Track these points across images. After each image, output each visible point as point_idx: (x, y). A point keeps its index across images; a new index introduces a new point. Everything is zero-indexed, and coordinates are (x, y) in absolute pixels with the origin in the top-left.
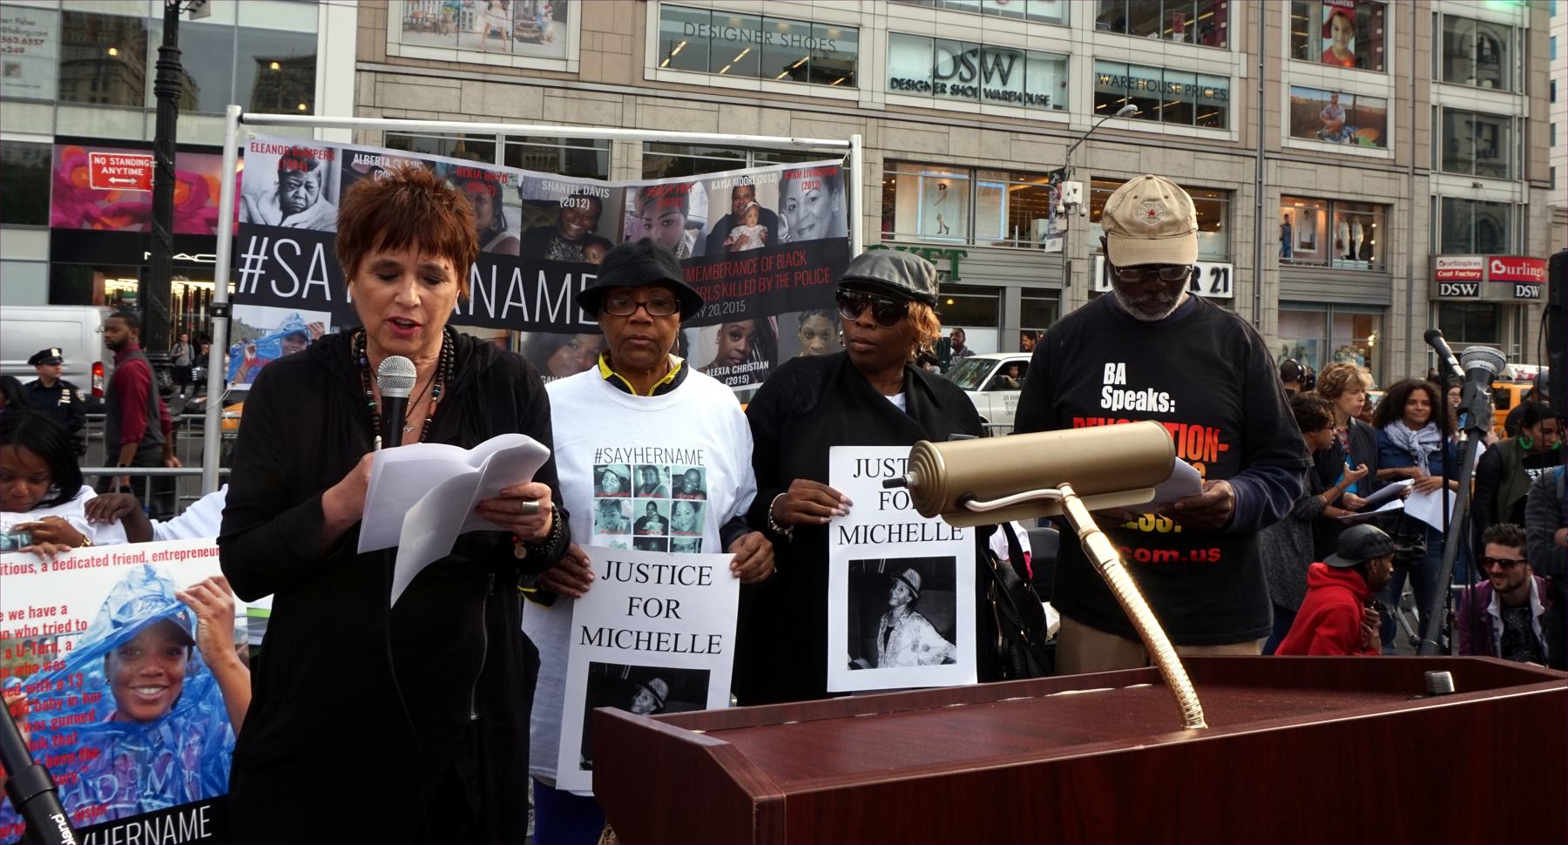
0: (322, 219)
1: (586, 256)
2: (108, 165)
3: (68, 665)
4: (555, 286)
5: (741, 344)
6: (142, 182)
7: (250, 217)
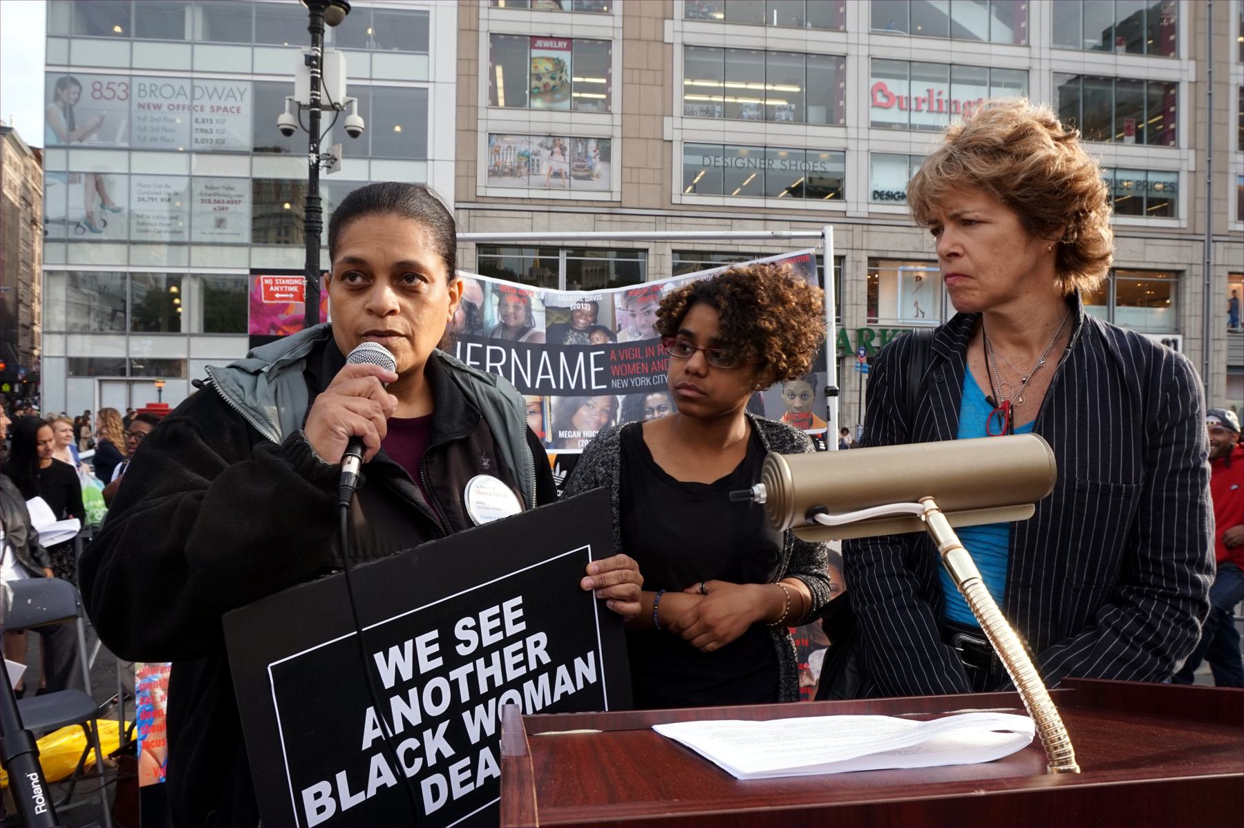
2: (274, 285)
6: (298, 297)
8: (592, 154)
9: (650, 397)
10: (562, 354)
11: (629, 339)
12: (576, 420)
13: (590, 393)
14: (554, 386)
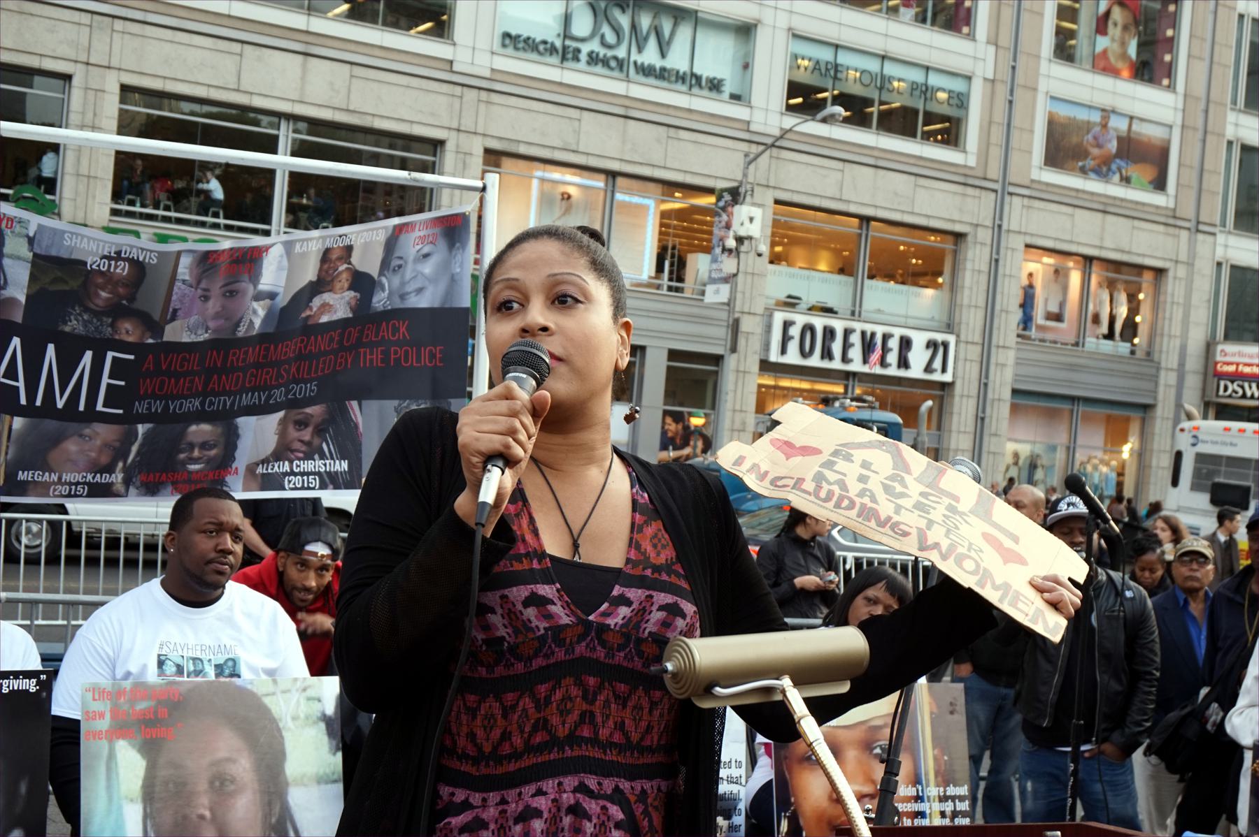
1: (115, 330)
4: (67, 365)
5: (307, 434)
13: (91, 416)
14: (23, 401)
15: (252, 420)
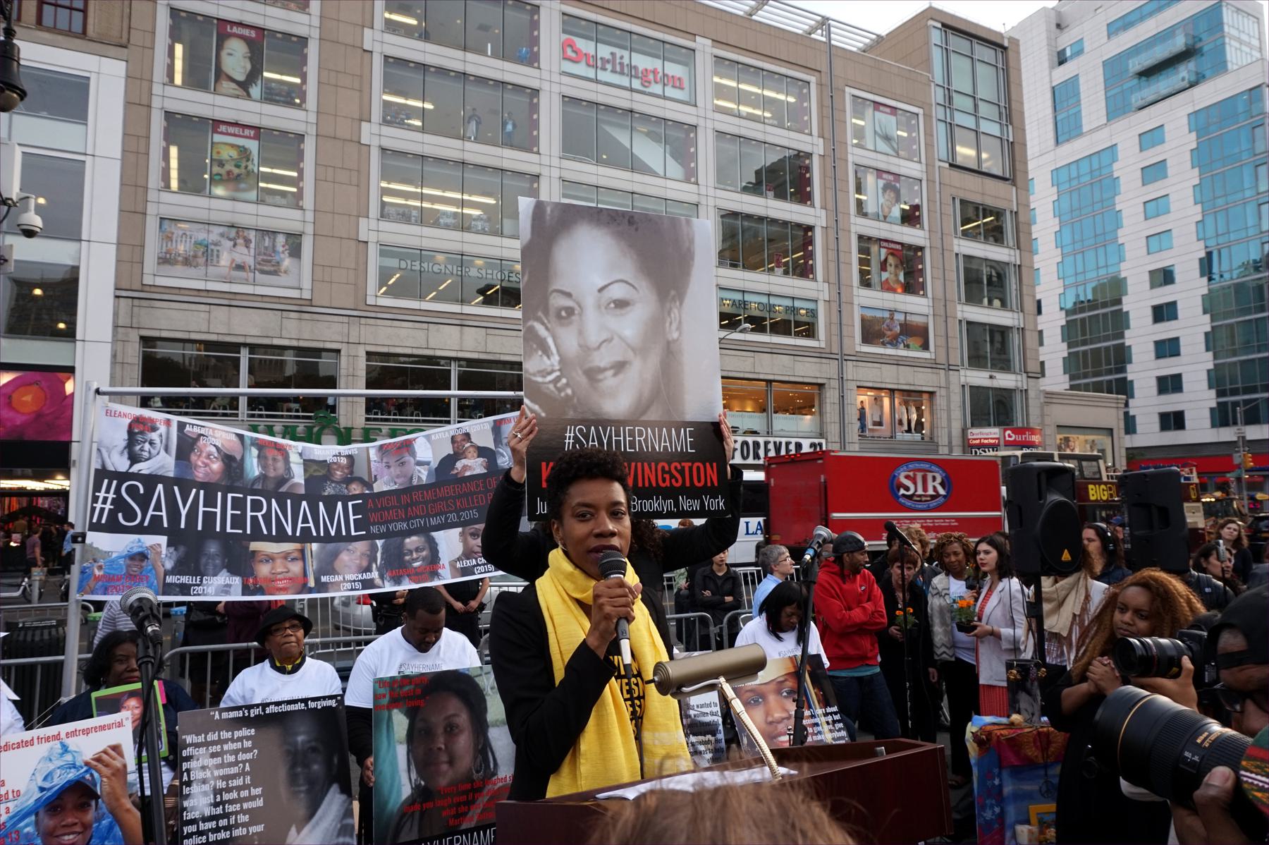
0: (162, 467)
3: (8, 825)
7: (103, 465)
8: (281, 249)
9: (407, 540)
10: (321, 504)
11: (385, 489)
12: (337, 565)
15: (442, 532)
